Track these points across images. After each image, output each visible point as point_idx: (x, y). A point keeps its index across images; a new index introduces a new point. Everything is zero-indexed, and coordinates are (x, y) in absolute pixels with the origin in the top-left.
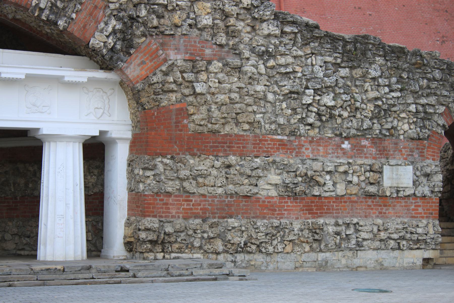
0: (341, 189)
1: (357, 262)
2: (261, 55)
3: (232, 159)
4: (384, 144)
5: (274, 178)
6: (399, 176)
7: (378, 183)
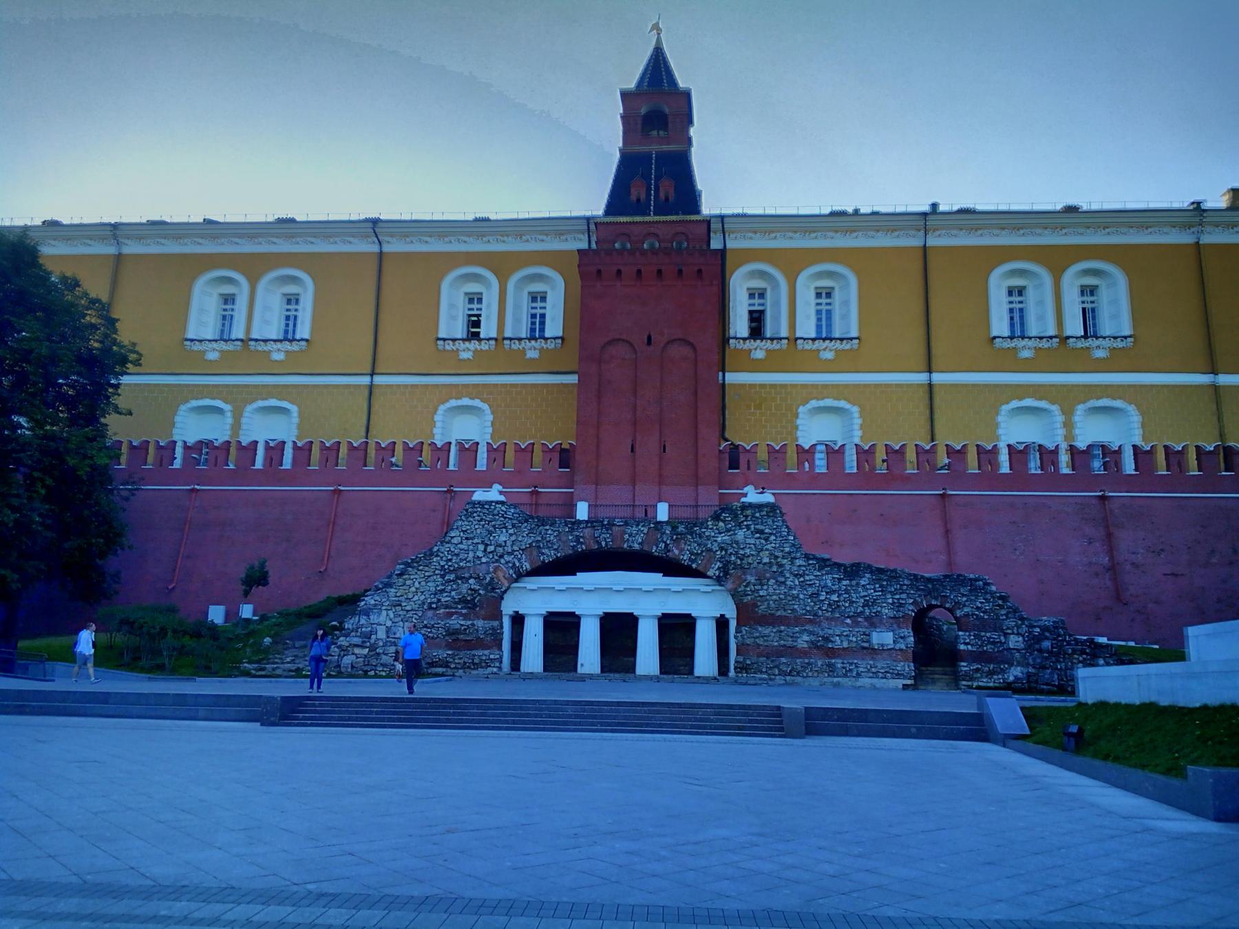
0: (845, 645)
1: (858, 684)
2: (796, 575)
3: (783, 628)
4: (873, 622)
5: (806, 638)
6: (883, 637)
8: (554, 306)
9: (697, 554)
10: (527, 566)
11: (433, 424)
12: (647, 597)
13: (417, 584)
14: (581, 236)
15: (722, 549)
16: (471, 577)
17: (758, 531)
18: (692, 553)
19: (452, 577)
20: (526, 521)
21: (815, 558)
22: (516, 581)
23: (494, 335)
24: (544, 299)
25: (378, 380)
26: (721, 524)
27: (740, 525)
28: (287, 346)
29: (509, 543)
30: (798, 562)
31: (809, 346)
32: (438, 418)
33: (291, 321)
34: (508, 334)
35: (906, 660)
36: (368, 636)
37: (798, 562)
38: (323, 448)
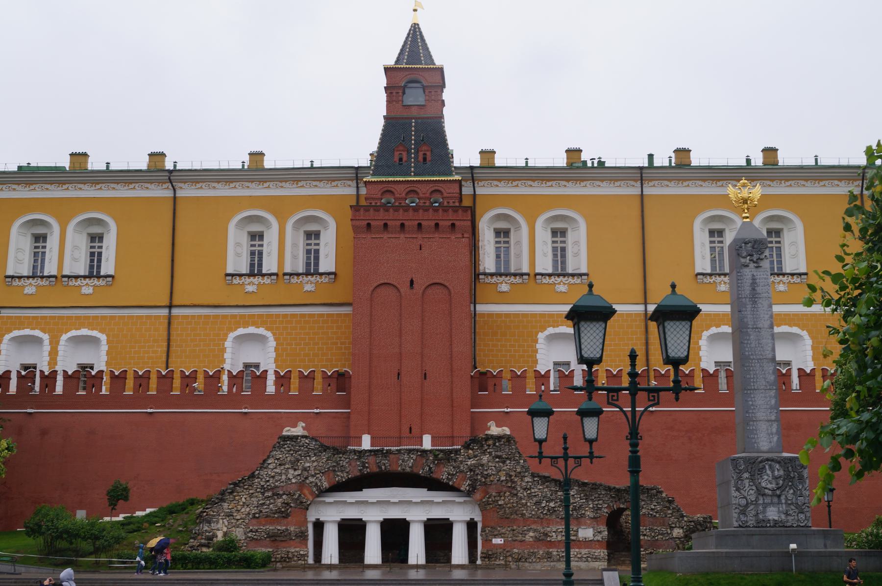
2: (525, 489)
5: (531, 534)
6: (586, 533)
7: (576, 535)
8: (326, 245)
9: (453, 475)
10: (326, 485)
11: (224, 350)
12: (416, 507)
13: (243, 500)
14: (350, 183)
15: (471, 470)
16: (284, 494)
17: (497, 457)
18: (449, 474)
19: (270, 494)
20: (325, 451)
21: (539, 476)
22: (318, 496)
23: (275, 270)
24: (317, 235)
25: (175, 311)
26: (470, 451)
27: (484, 453)
28: (96, 282)
29: (312, 469)
30: (527, 479)
31: (546, 280)
32: (228, 344)
33: (95, 258)
34: (288, 269)
35: (601, 548)
36: (210, 539)
37: (527, 479)
38: (137, 376)
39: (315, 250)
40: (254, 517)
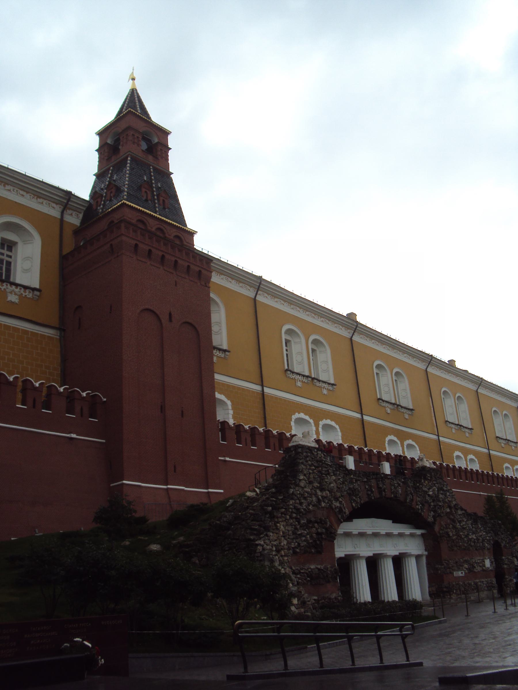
7: (485, 566)
13: (282, 527)
15: (433, 501)
26: (426, 482)
39: (7, 261)
40: (295, 553)
